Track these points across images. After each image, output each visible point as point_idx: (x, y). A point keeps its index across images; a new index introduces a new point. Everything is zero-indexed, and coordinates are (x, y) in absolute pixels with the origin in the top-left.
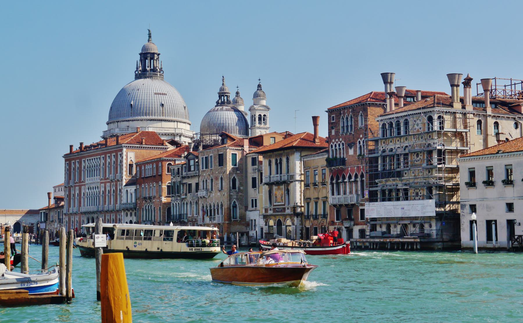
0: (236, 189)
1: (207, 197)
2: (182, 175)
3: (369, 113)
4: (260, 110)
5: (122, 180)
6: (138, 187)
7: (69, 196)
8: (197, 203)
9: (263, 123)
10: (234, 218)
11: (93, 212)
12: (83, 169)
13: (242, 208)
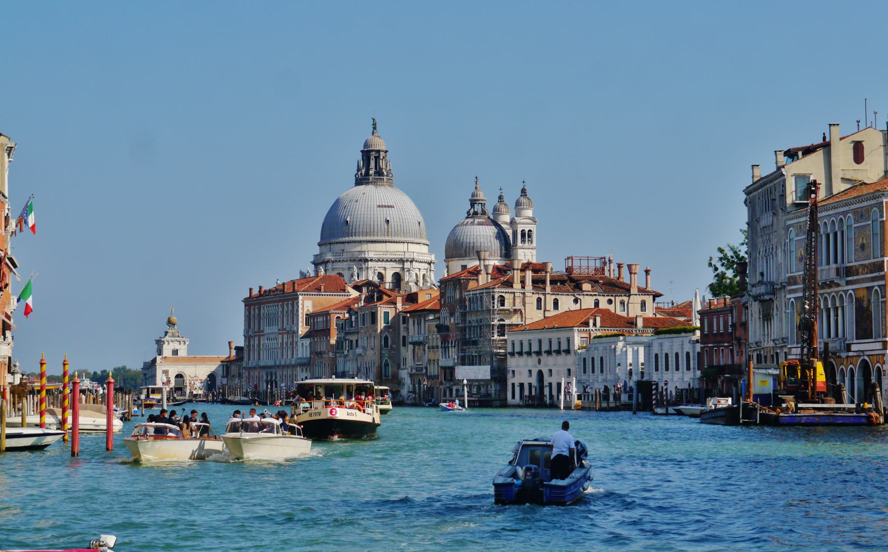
1: (363, 355)
4: (524, 224)
5: (298, 332)
7: (249, 346)
8: (357, 360)
9: (529, 241)
10: (387, 375)
11: (271, 367)
12: (262, 316)
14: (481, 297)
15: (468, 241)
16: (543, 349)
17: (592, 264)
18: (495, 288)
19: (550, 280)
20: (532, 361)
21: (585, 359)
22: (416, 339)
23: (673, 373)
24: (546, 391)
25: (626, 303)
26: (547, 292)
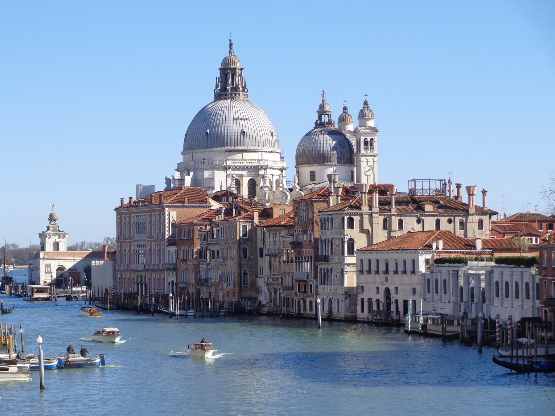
3: (314, 208)
4: (366, 133)
7: (121, 251)
8: (218, 268)
9: (371, 148)
10: (246, 283)
11: (141, 271)
13: (252, 275)
14: (332, 218)
17: (433, 186)
18: (344, 210)
19: (396, 202)
20: (379, 279)
21: (429, 280)
22: (272, 252)
23: (512, 300)
24: (393, 307)
26: (392, 213)
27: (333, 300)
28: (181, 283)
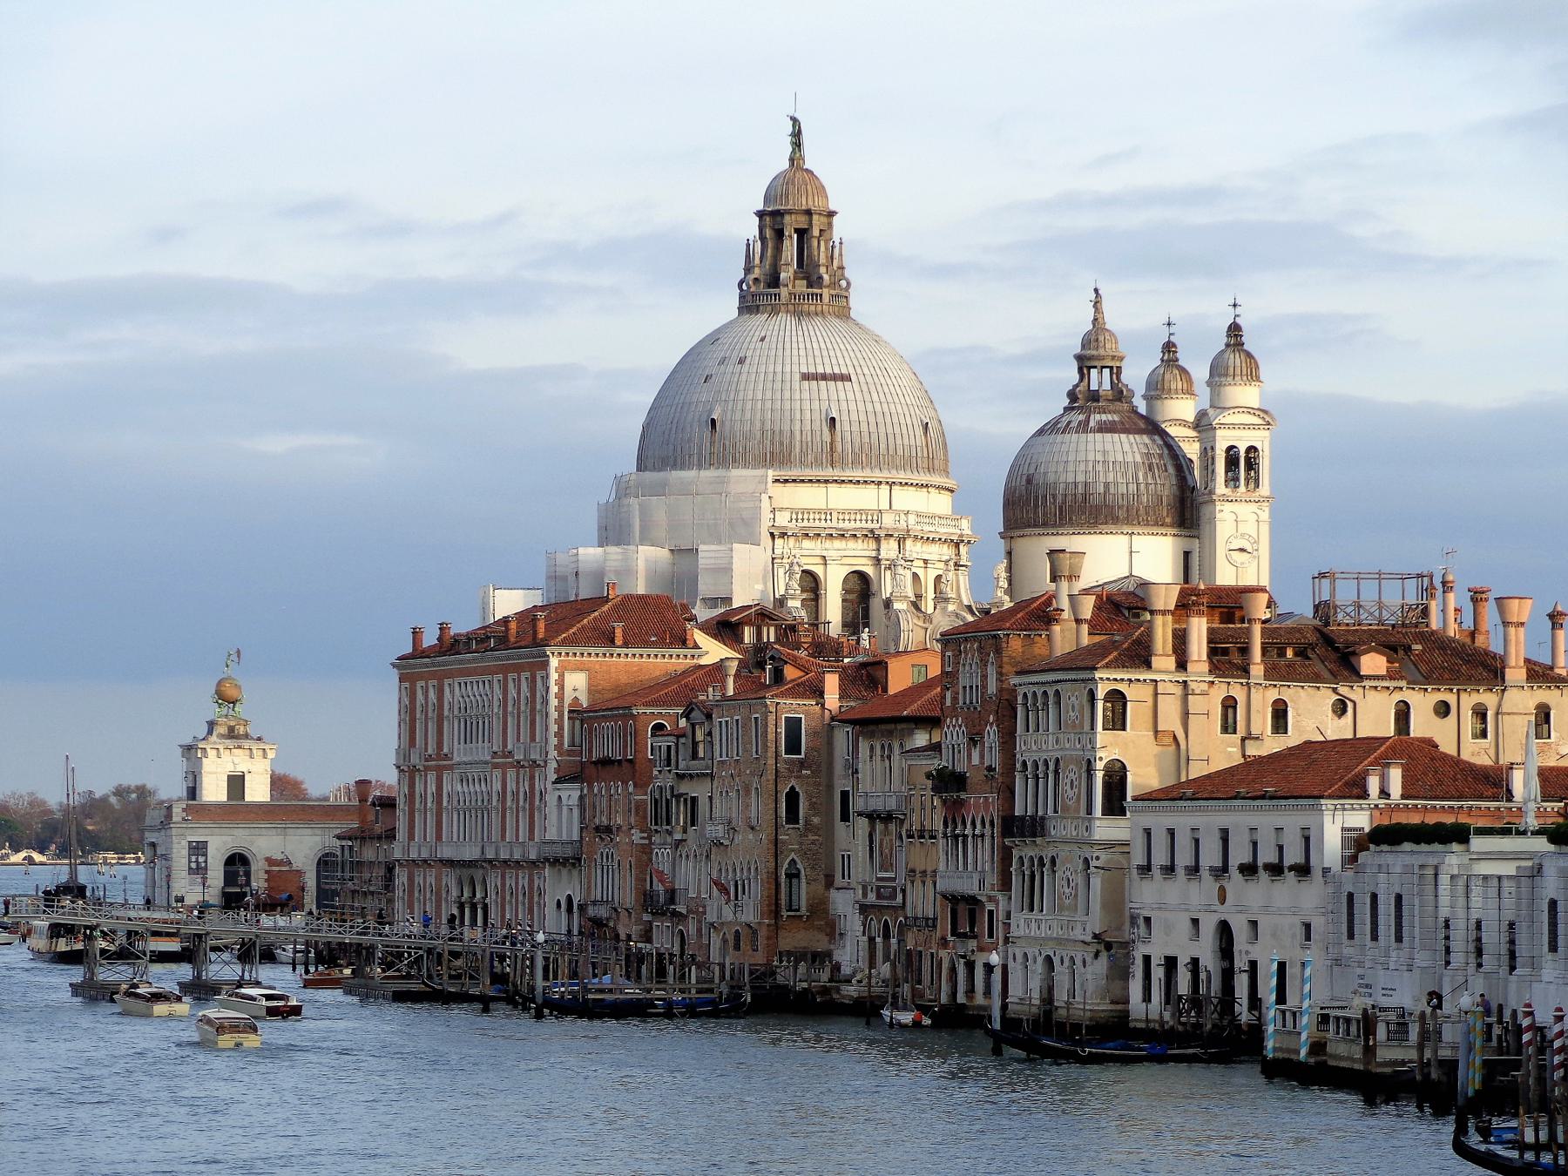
0: (798, 823)
1: (726, 842)
2: (677, 768)
3: (1005, 659)
4: (1233, 426)
6: (585, 791)
10: (794, 908)
11: (471, 864)
12: (446, 713)
13: (814, 880)
14: (1057, 693)
15: (1071, 479)
16: (1234, 862)
21: (1350, 896)
22: (876, 804)
25: (1490, 714)
27: (1056, 961)
28: (594, 903)
